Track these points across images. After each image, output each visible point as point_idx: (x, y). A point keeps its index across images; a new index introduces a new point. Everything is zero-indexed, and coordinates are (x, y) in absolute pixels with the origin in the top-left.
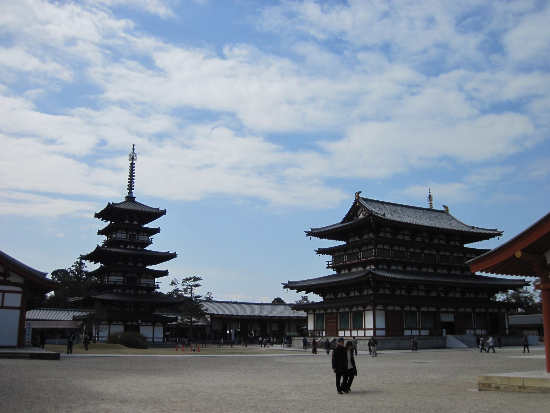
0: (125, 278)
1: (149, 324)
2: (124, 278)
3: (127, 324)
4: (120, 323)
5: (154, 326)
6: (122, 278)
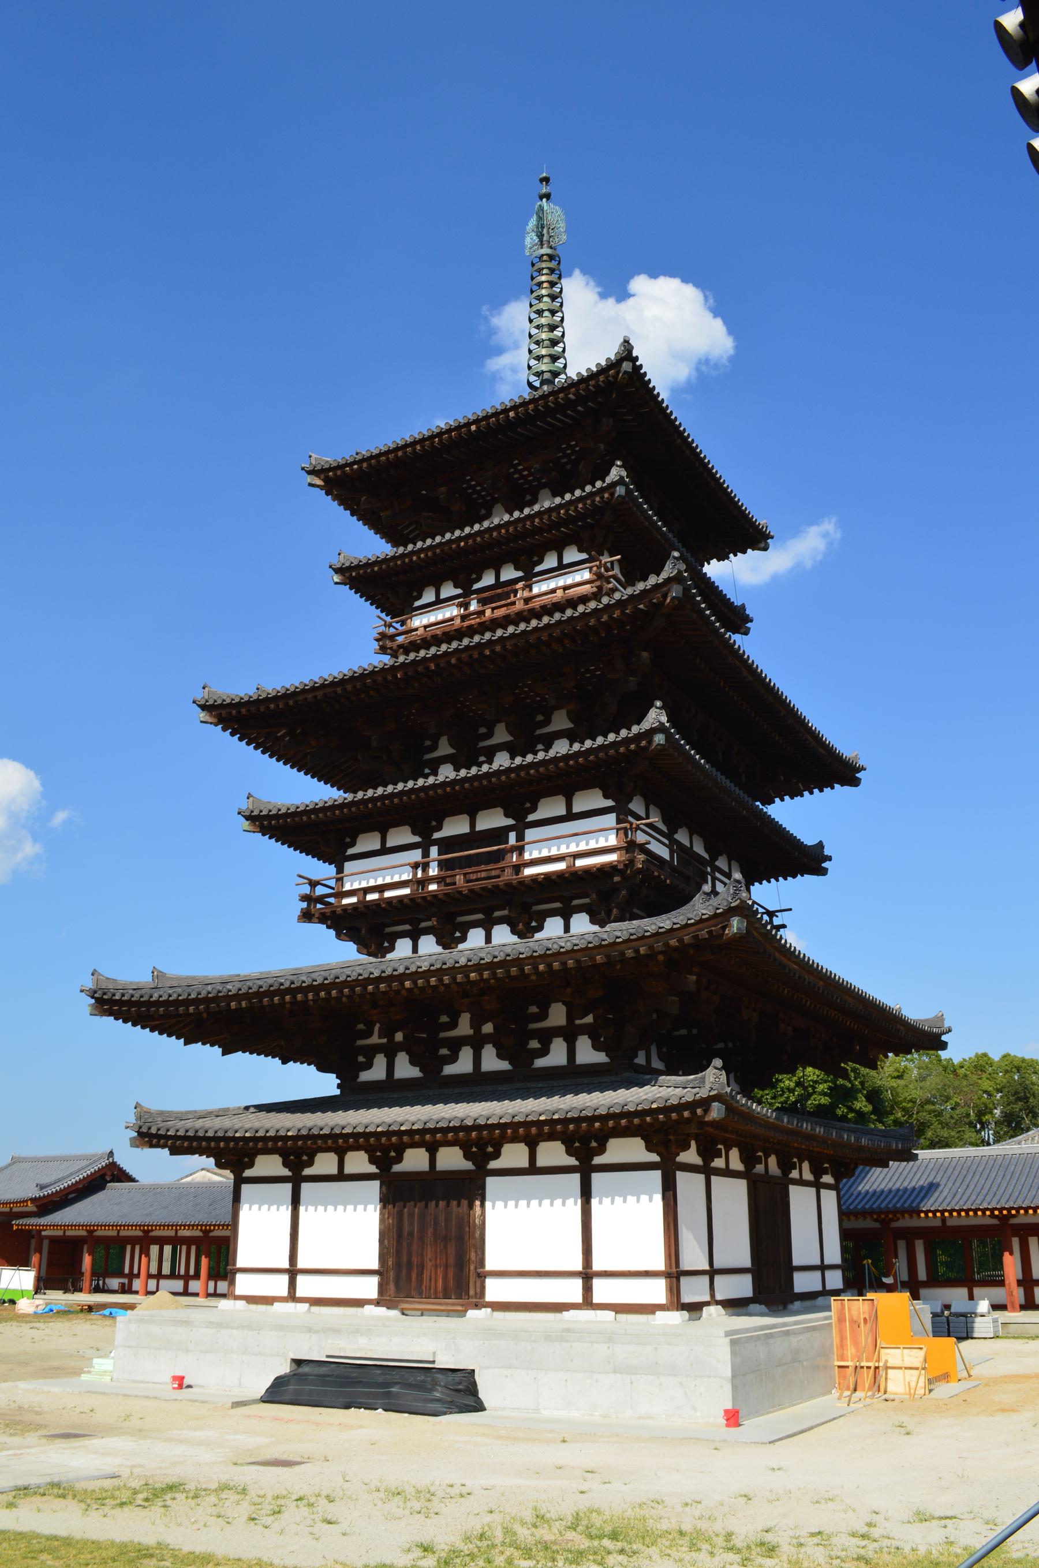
0: (434, 851)
1: (552, 1153)
2: (426, 854)
3: (397, 1168)
4: (358, 1162)
5: (586, 1171)
6: (416, 855)
